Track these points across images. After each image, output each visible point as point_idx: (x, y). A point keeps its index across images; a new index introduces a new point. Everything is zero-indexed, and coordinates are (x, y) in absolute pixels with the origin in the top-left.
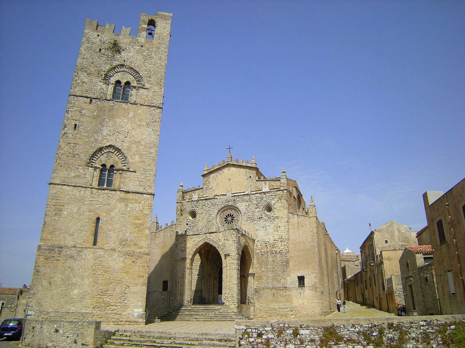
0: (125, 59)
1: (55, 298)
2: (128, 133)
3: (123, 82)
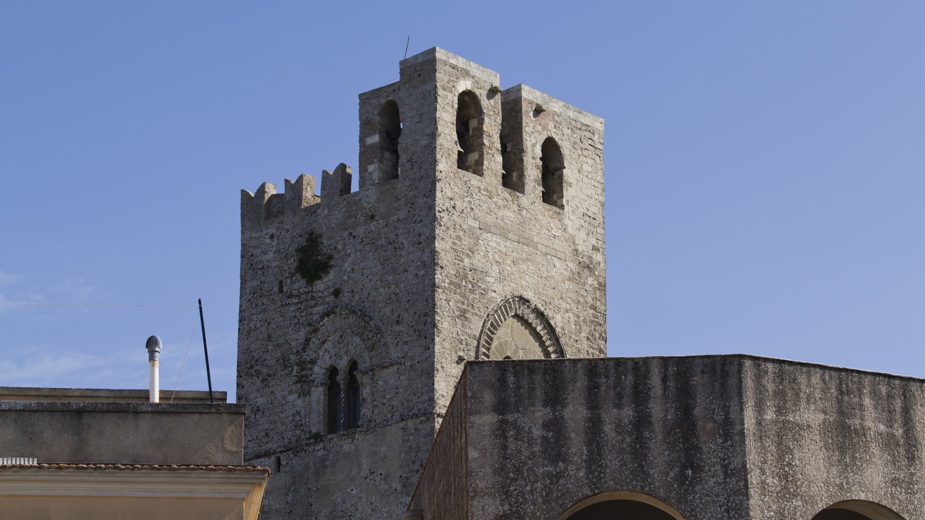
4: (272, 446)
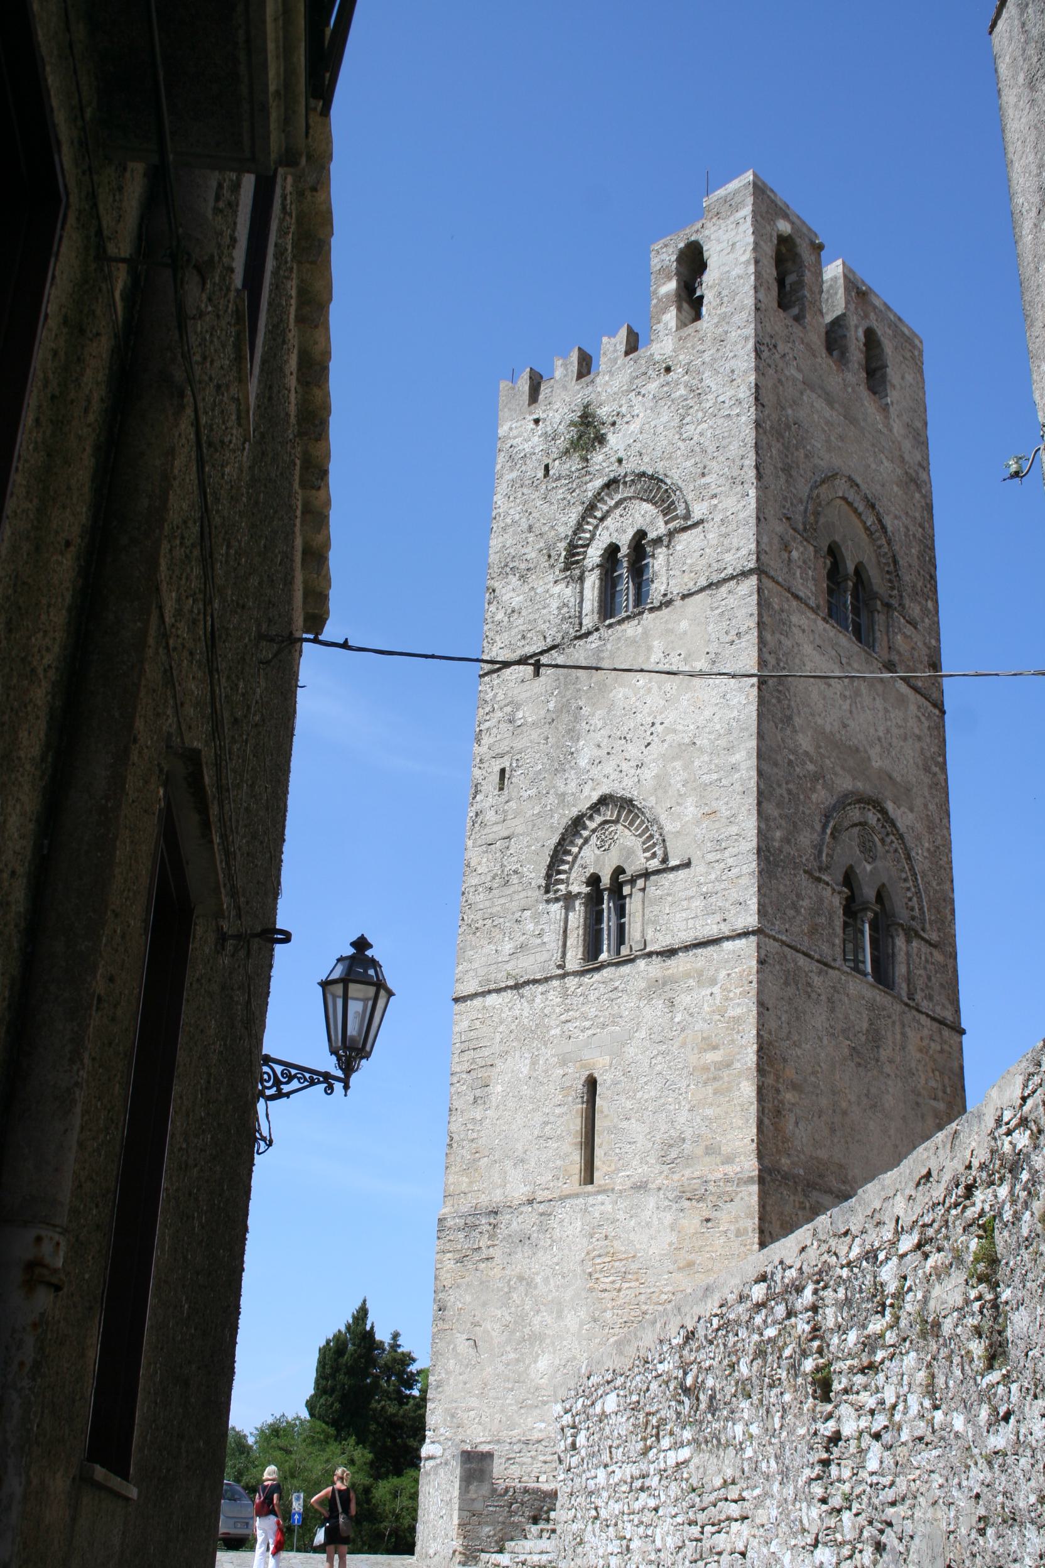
0: (621, 454)
1: (492, 1394)
2: (653, 724)
3: (624, 541)
4: (529, 650)
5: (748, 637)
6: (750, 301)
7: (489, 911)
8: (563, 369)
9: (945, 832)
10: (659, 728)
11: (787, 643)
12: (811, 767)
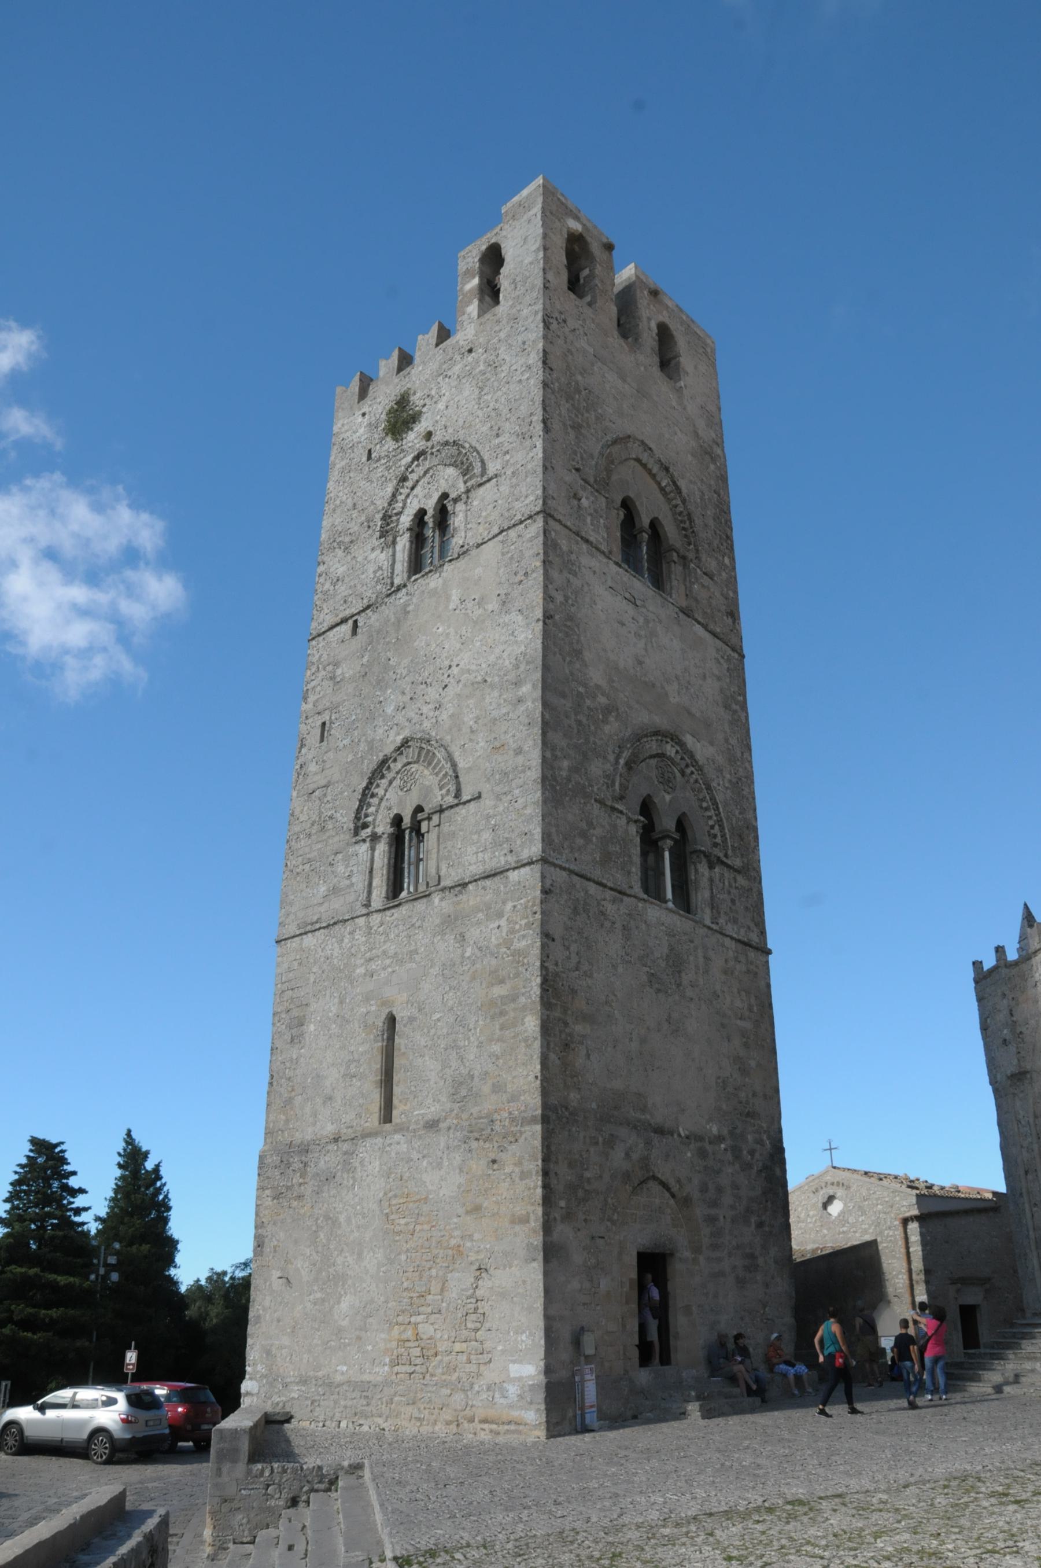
2: (450, 667)
4: (348, 613)
5: (534, 575)
6: (539, 282)
7: (308, 856)
8: (387, 366)
9: (747, 765)
10: (455, 670)
11: (576, 582)
12: (602, 700)
